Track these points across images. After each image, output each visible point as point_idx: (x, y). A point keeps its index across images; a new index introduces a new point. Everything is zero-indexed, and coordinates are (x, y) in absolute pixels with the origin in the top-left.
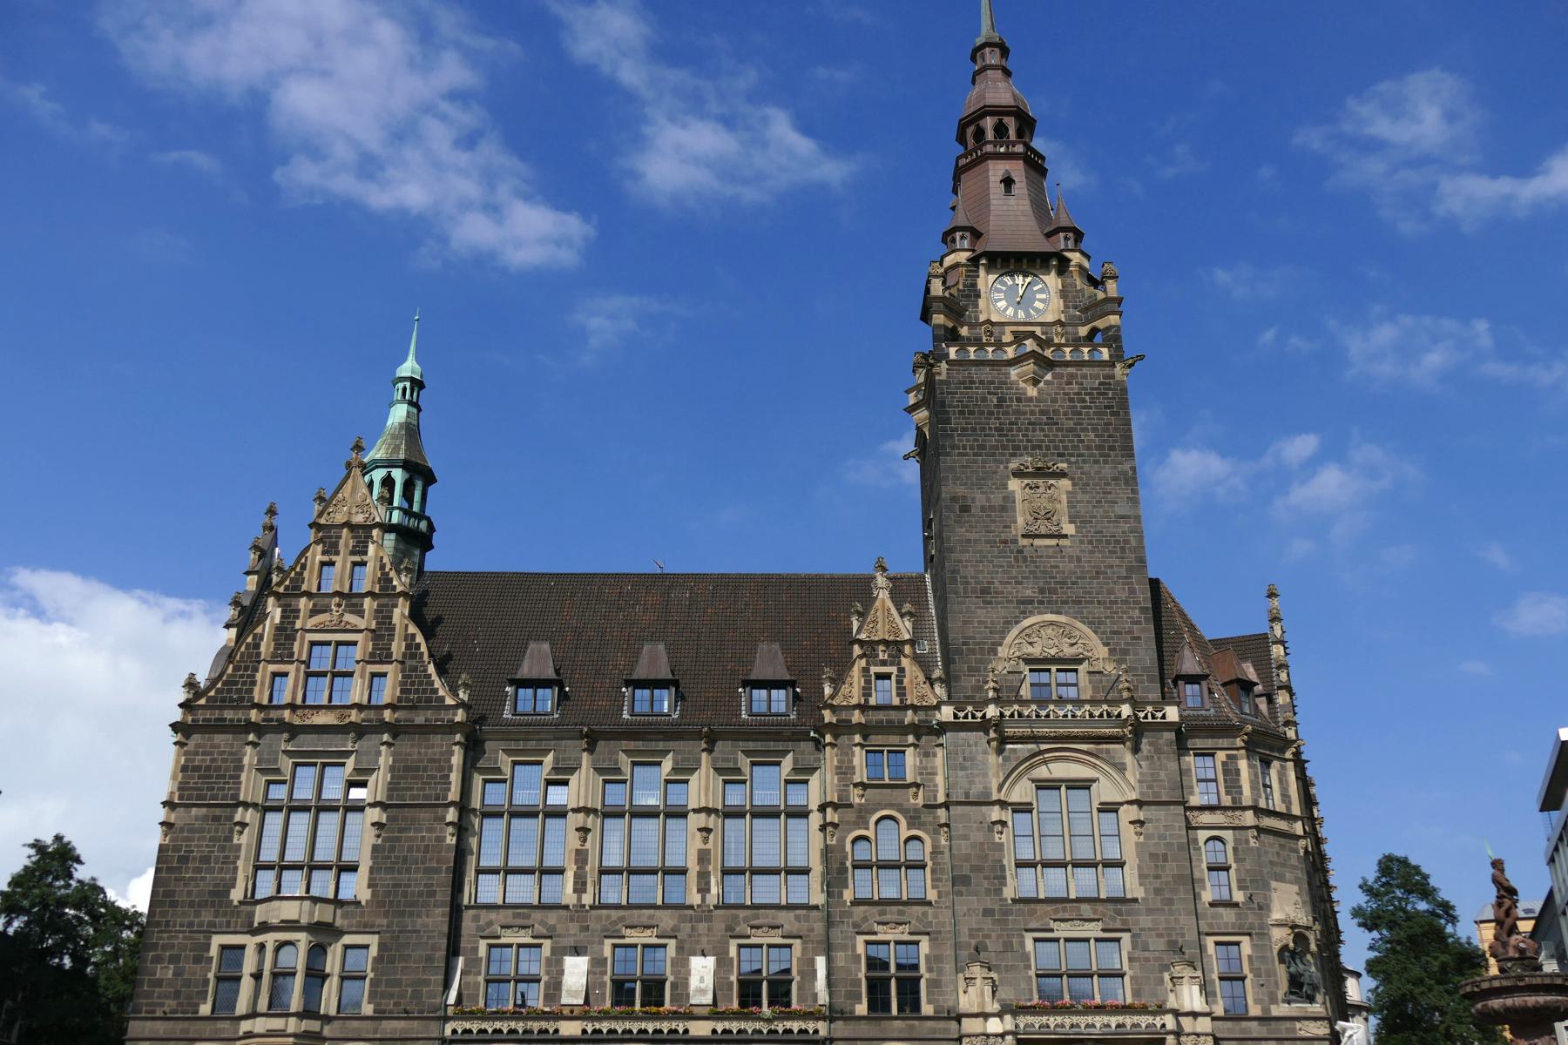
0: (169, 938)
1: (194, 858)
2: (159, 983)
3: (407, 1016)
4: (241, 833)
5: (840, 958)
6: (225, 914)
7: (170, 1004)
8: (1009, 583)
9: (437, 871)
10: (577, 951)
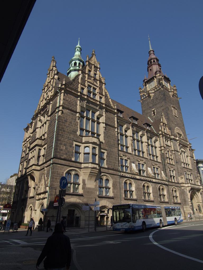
1: (68, 122)
2: (62, 150)
6: (76, 137)
7: (64, 156)
9: (115, 140)
10: (133, 163)
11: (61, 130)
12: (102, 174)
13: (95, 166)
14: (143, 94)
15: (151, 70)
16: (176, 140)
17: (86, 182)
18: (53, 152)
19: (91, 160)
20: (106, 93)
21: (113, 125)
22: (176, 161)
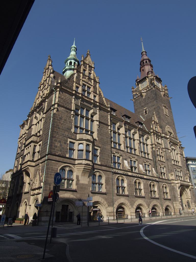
0: (58, 136)
2: (56, 146)
3: (106, 166)
6: (70, 134)
9: (108, 138)
10: (126, 160)
11: (56, 127)
12: (96, 170)
13: (89, 162)
14: (135, 93)
15: (143, 70)
16: (167, 138)
17: (80, 179)
18: (48, 148)
19: (84, 157)
20: (100, 92)
21: (106, 123)
22: (167, 158)
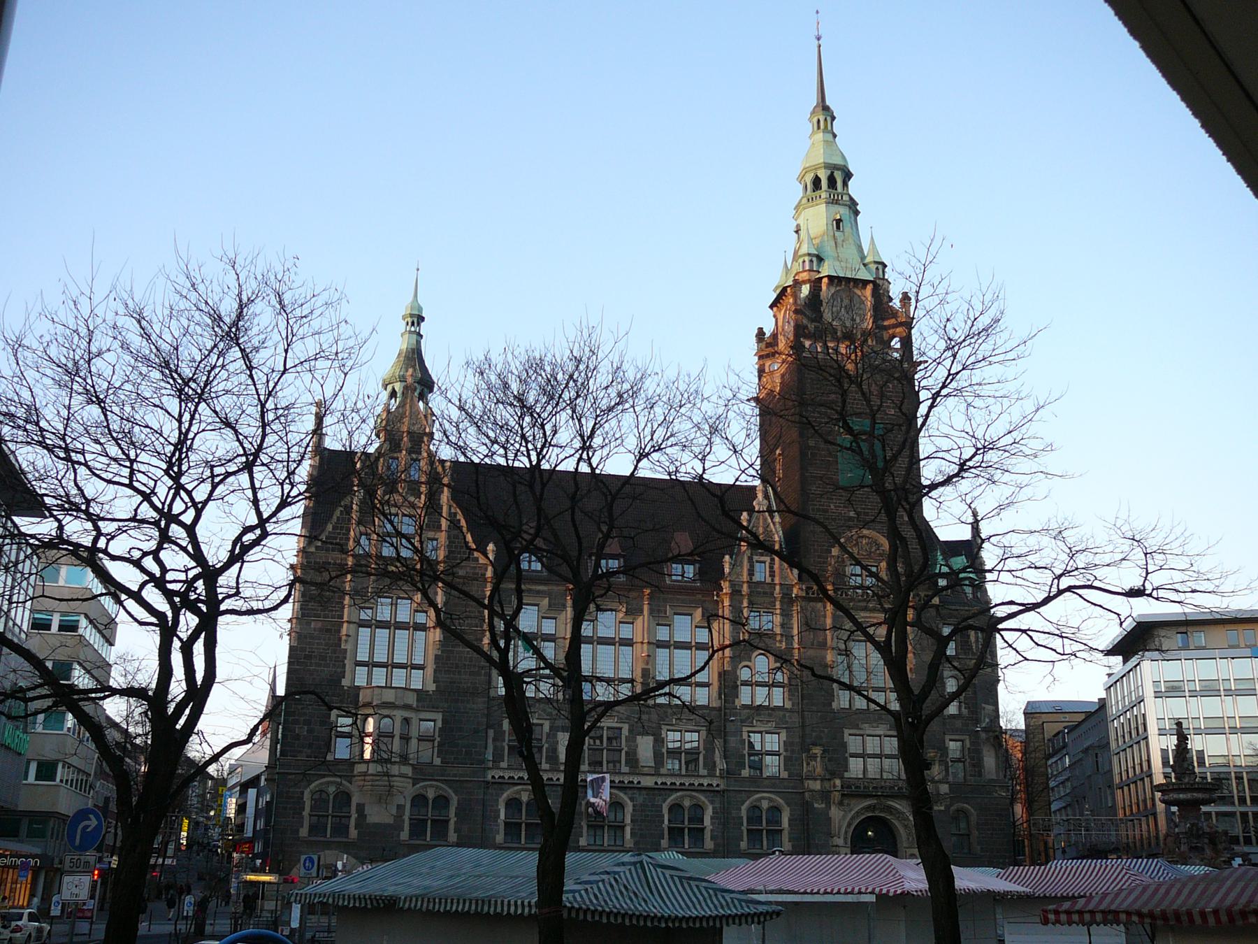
0: (302, 709)
1: (315, 657)
4: (346, 641)
5: (733, 741)
8: (840, 507)
17: (367, 810)
20: (452, 516)
